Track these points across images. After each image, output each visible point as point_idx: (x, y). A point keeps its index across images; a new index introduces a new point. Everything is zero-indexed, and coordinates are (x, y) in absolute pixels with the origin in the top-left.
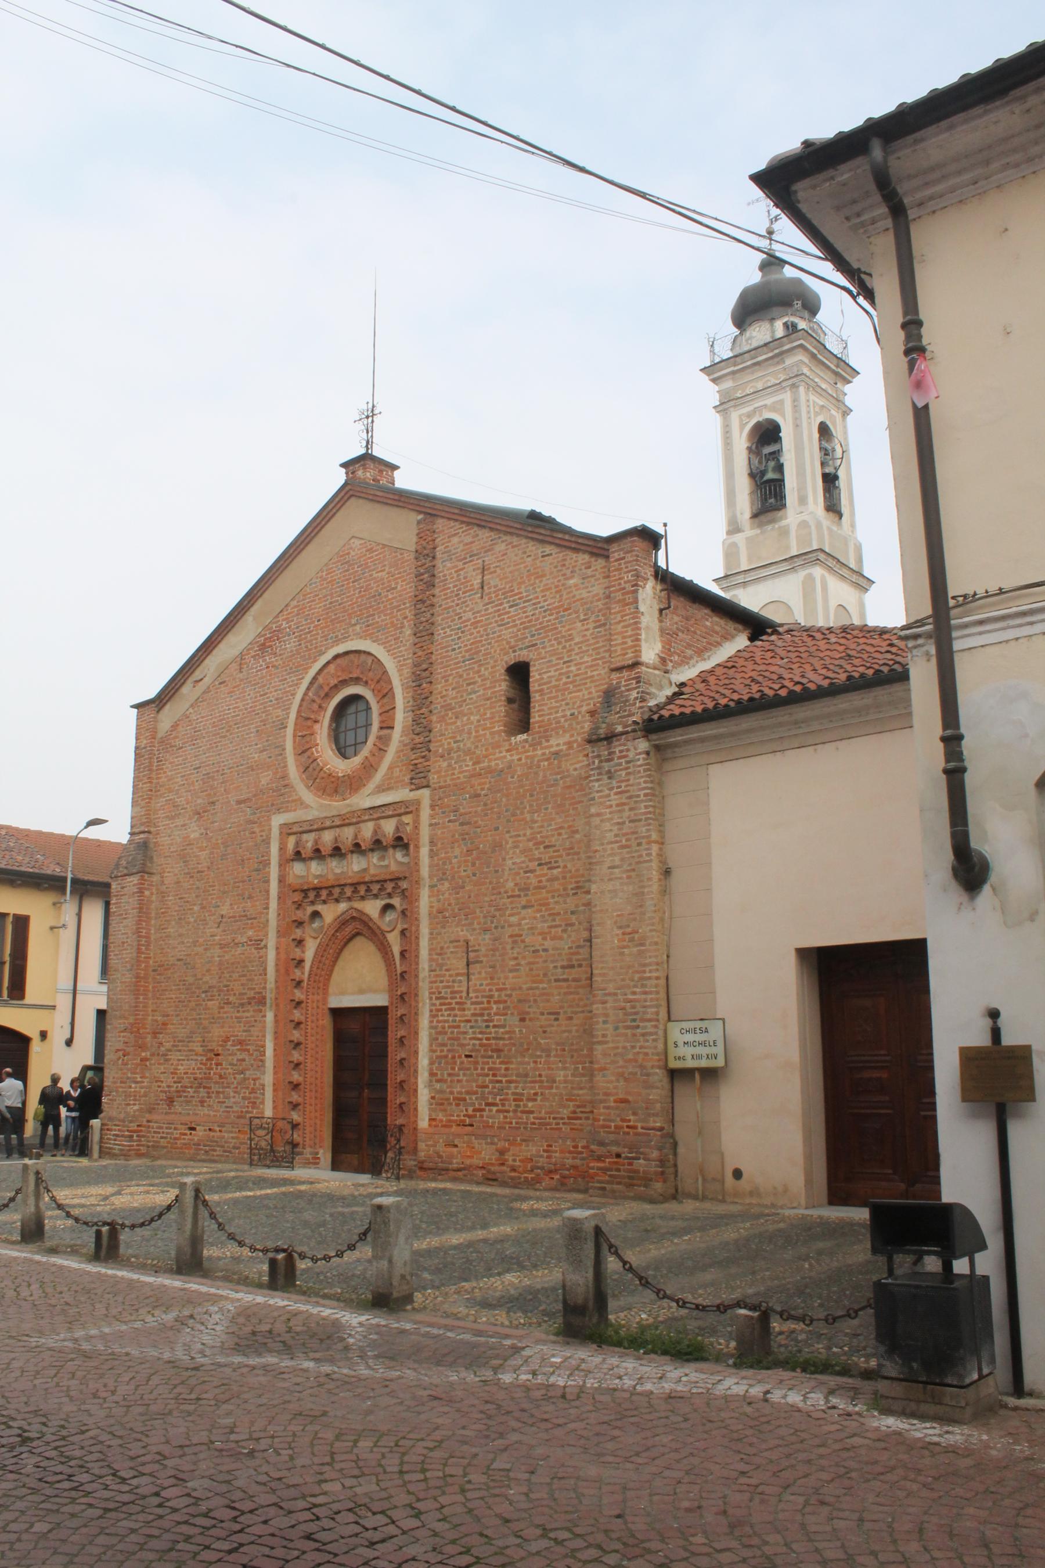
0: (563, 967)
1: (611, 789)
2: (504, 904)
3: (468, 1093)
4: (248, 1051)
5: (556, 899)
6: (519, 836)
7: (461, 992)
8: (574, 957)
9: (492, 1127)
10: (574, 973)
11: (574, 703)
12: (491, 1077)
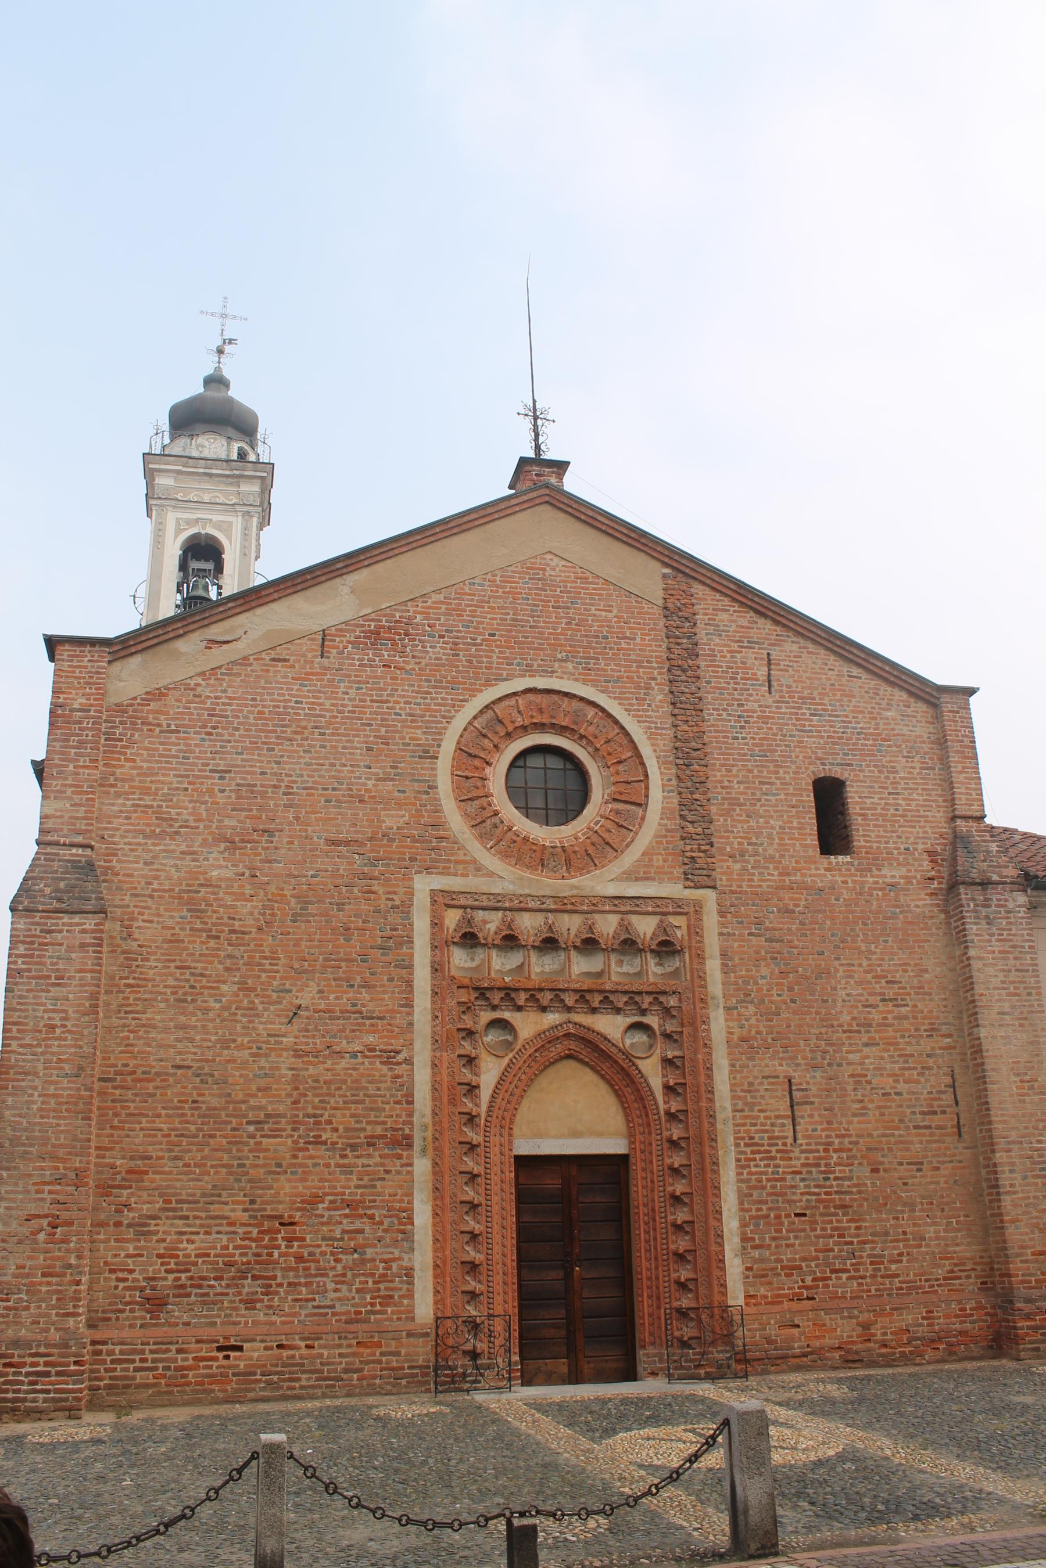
0: (922, 1113)
1: (992, 935)
2: (840, 1039)
3: (804, 1259)
4: (372, 1217)
5: (907, 1039)
6: (853, 965)
7: (786, 1137)
8: (936, 1103)
9: (845, 1298)
10: (937, 1120)
11: (907, 838)
12: (836, 1238)
